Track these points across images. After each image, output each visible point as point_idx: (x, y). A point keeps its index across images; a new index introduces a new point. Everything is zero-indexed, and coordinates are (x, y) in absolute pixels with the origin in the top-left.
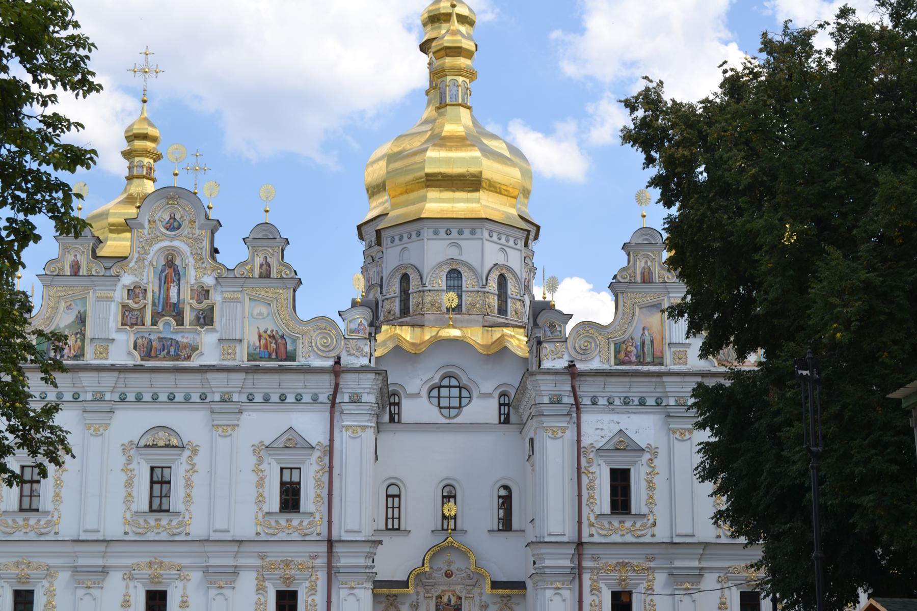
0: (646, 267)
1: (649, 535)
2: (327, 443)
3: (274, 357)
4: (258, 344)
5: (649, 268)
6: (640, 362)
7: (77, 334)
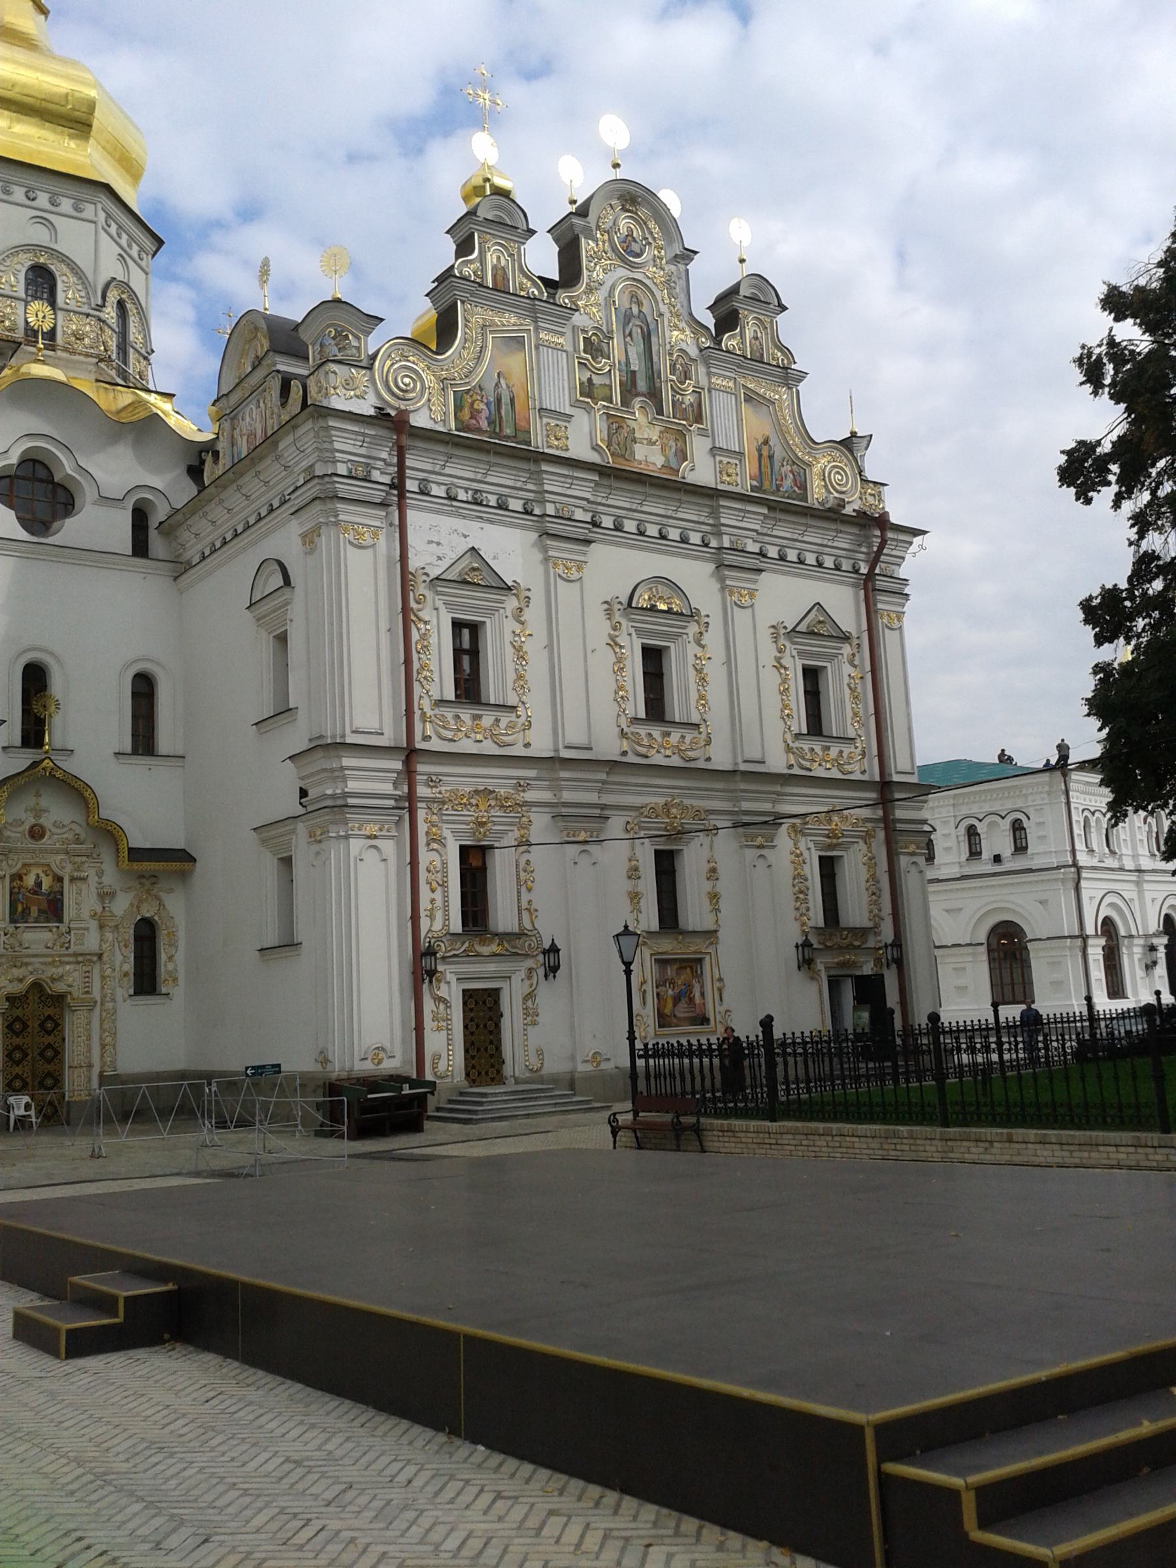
1: (520, 744)
6: (494, 432)
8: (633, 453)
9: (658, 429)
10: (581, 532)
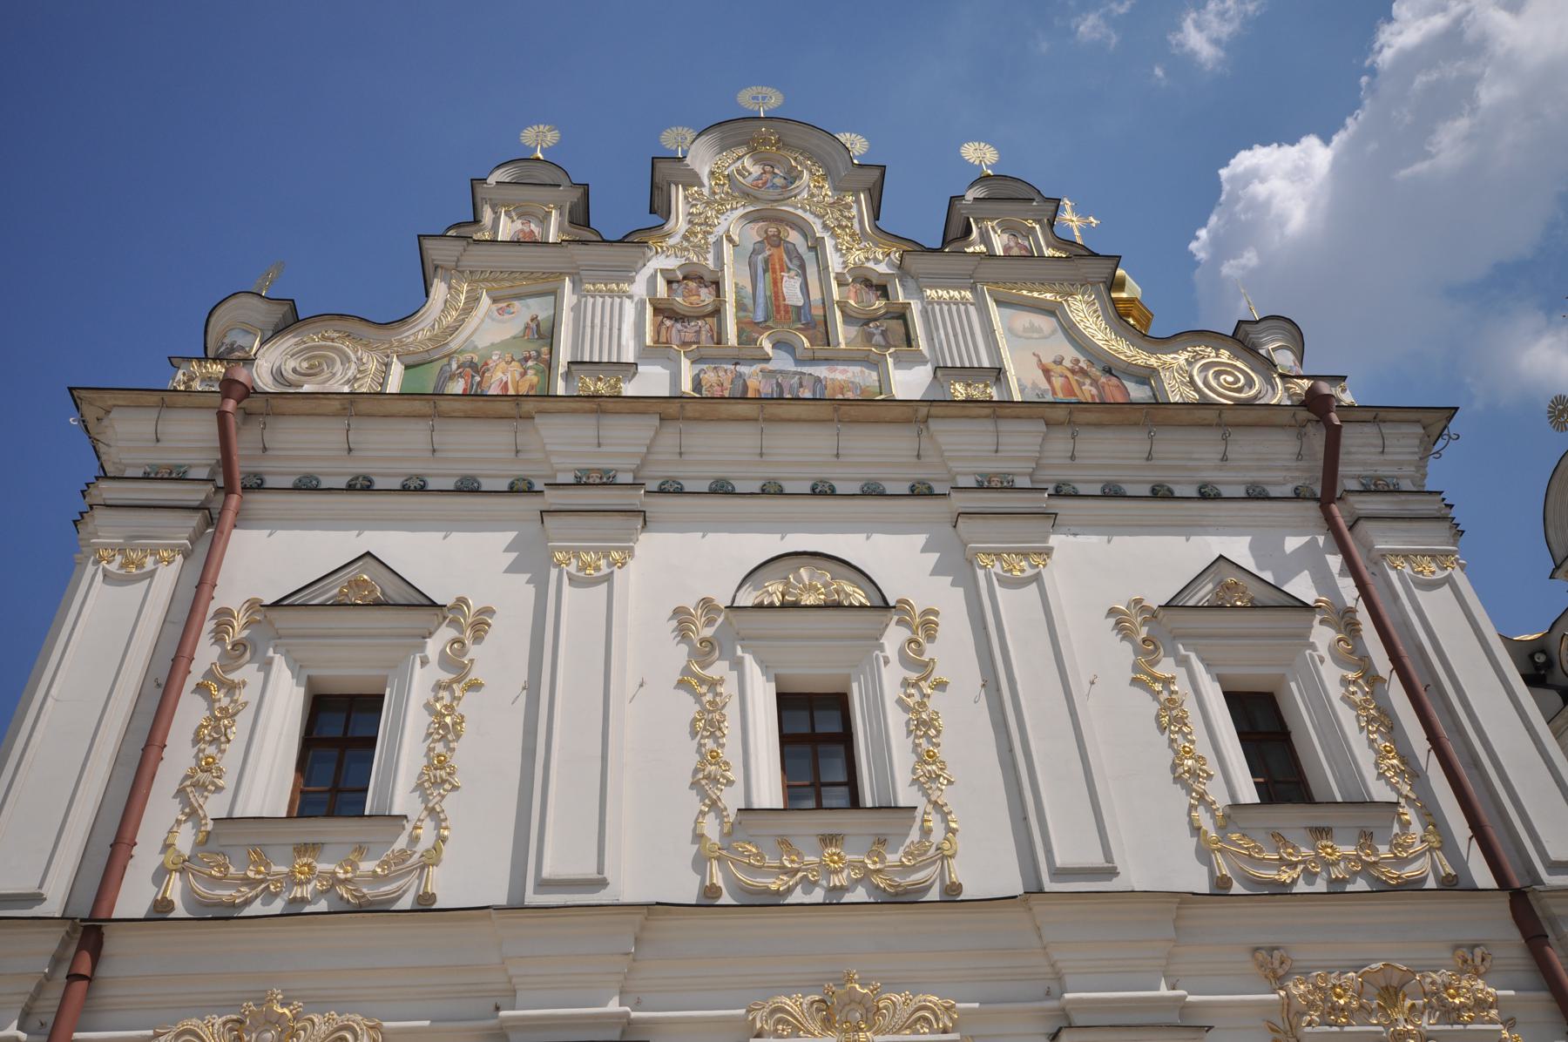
4: (1045, 385)
7: (526, 359)
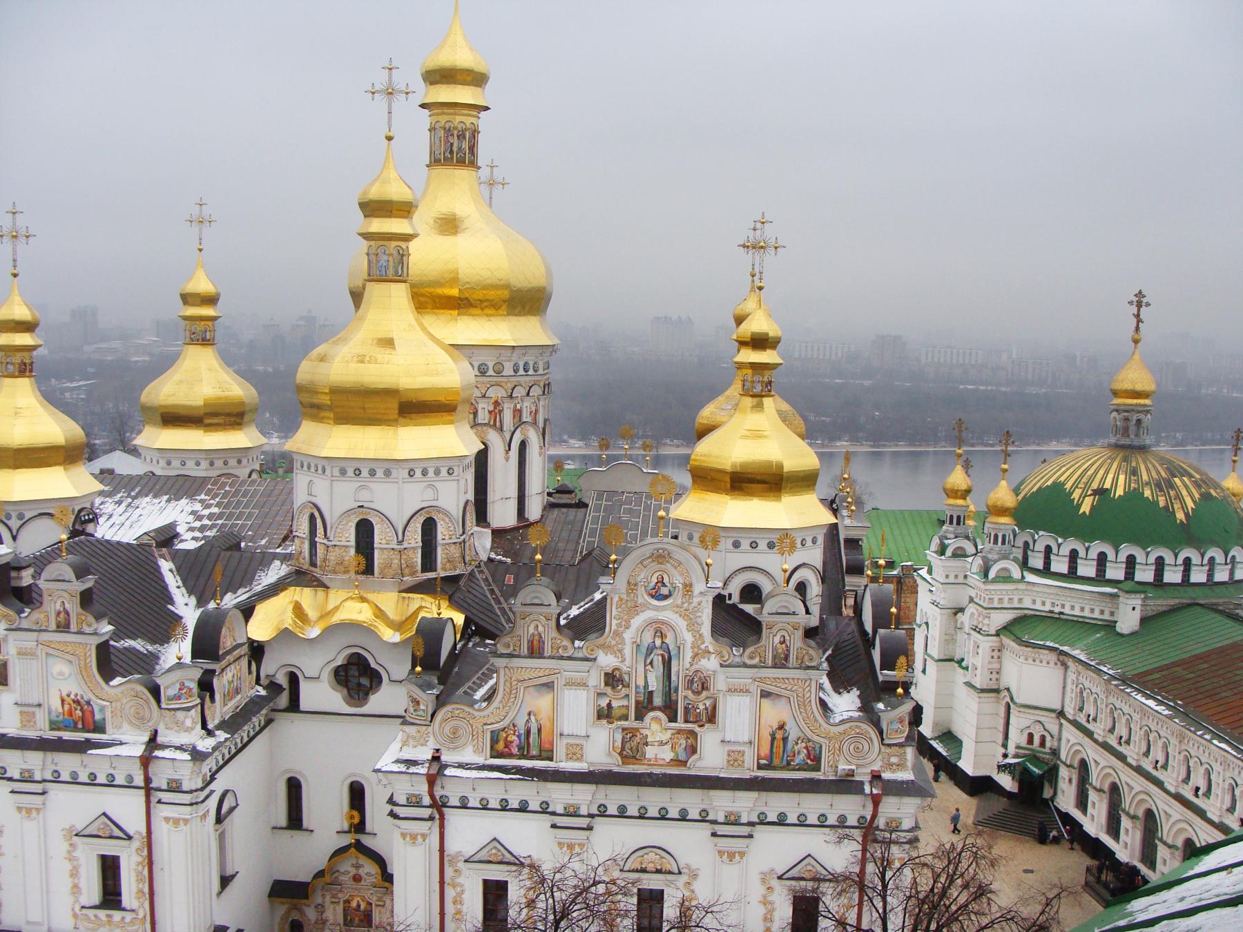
0: (536, 633)
2: (144, 831)
3: (80, 726)
5: (540, 634)
6: (523, 755)
8: (644, 754)
9: (669, 732)
10: (583, 822)
